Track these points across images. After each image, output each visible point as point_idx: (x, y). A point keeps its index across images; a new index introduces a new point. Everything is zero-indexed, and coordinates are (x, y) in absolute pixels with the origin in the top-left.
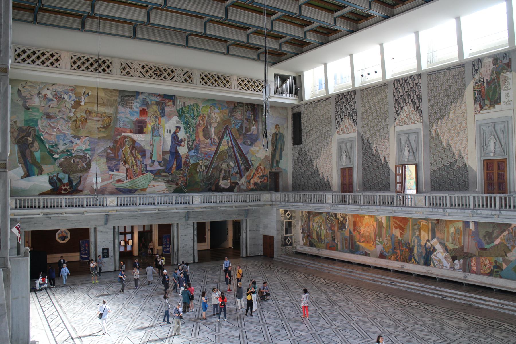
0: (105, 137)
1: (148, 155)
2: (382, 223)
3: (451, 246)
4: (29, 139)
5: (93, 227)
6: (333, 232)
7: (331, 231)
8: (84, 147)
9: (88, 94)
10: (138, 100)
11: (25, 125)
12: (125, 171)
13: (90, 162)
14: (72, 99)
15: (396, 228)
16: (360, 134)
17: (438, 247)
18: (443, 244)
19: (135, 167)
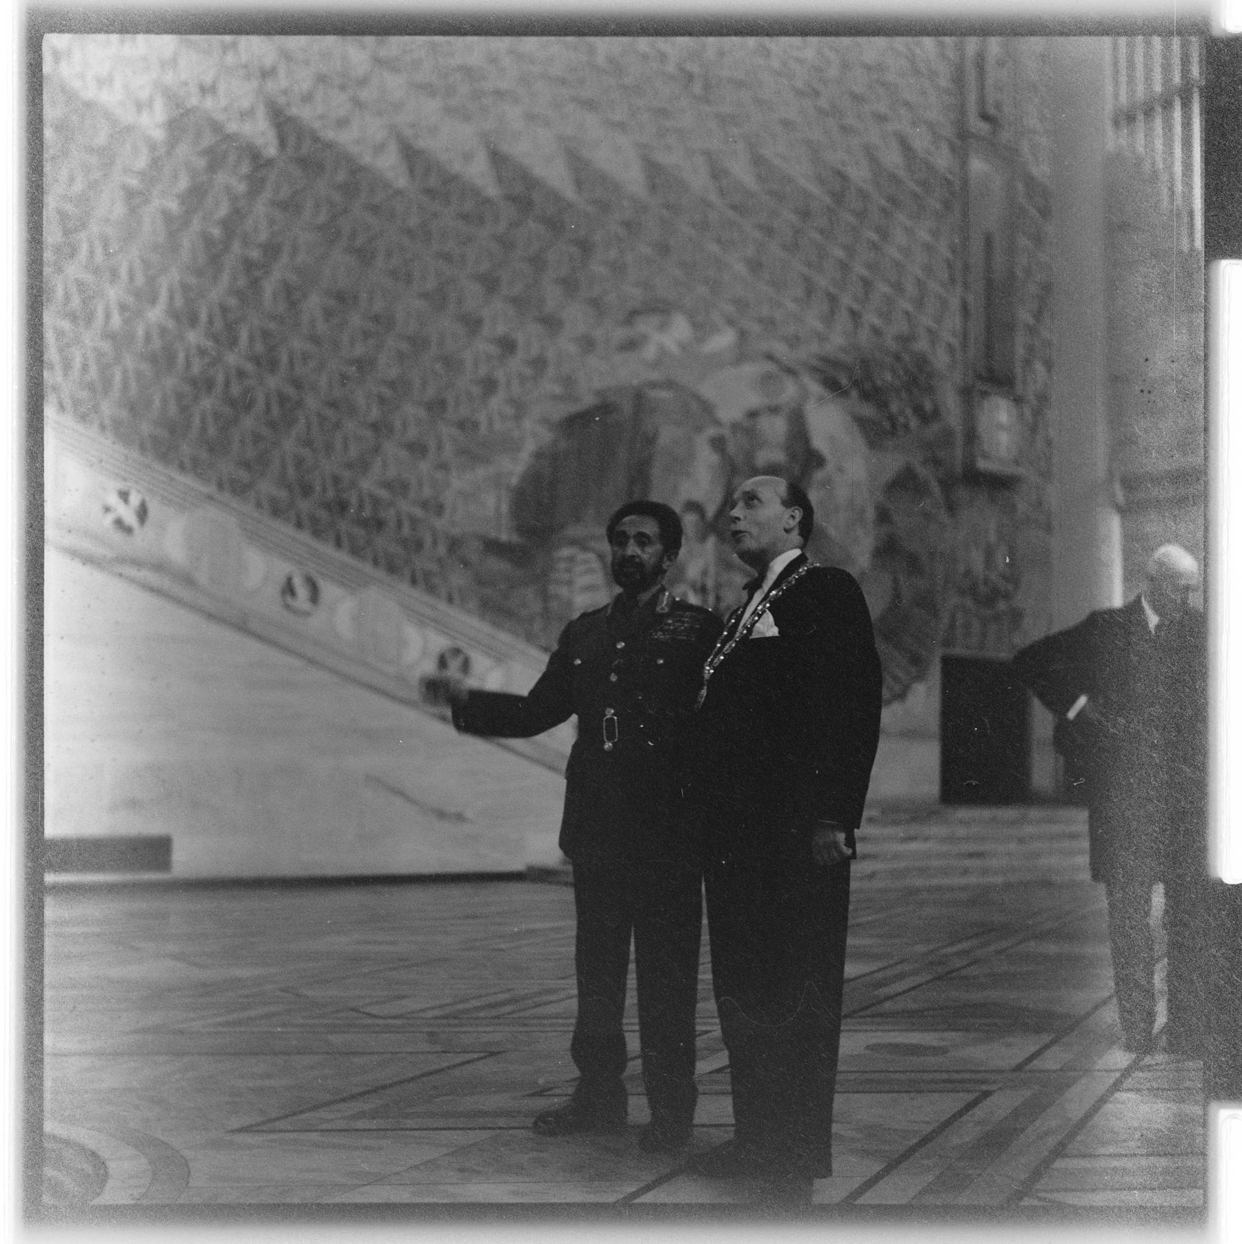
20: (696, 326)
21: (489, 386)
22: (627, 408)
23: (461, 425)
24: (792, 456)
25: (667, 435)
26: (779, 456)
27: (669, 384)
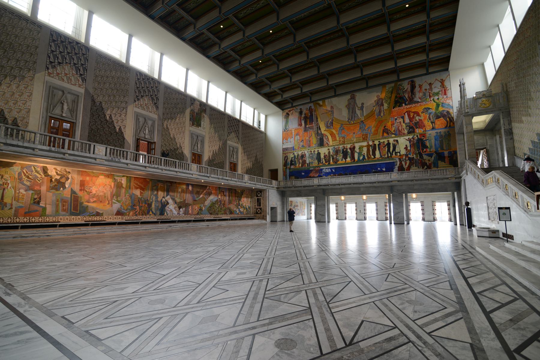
2: (122, 184)
3: (178, 200)
6: (39, 193)
7: (31, 192)
15: (136, 188)
16: (90, 94)
17: (170, 201)
18: (173, 199)
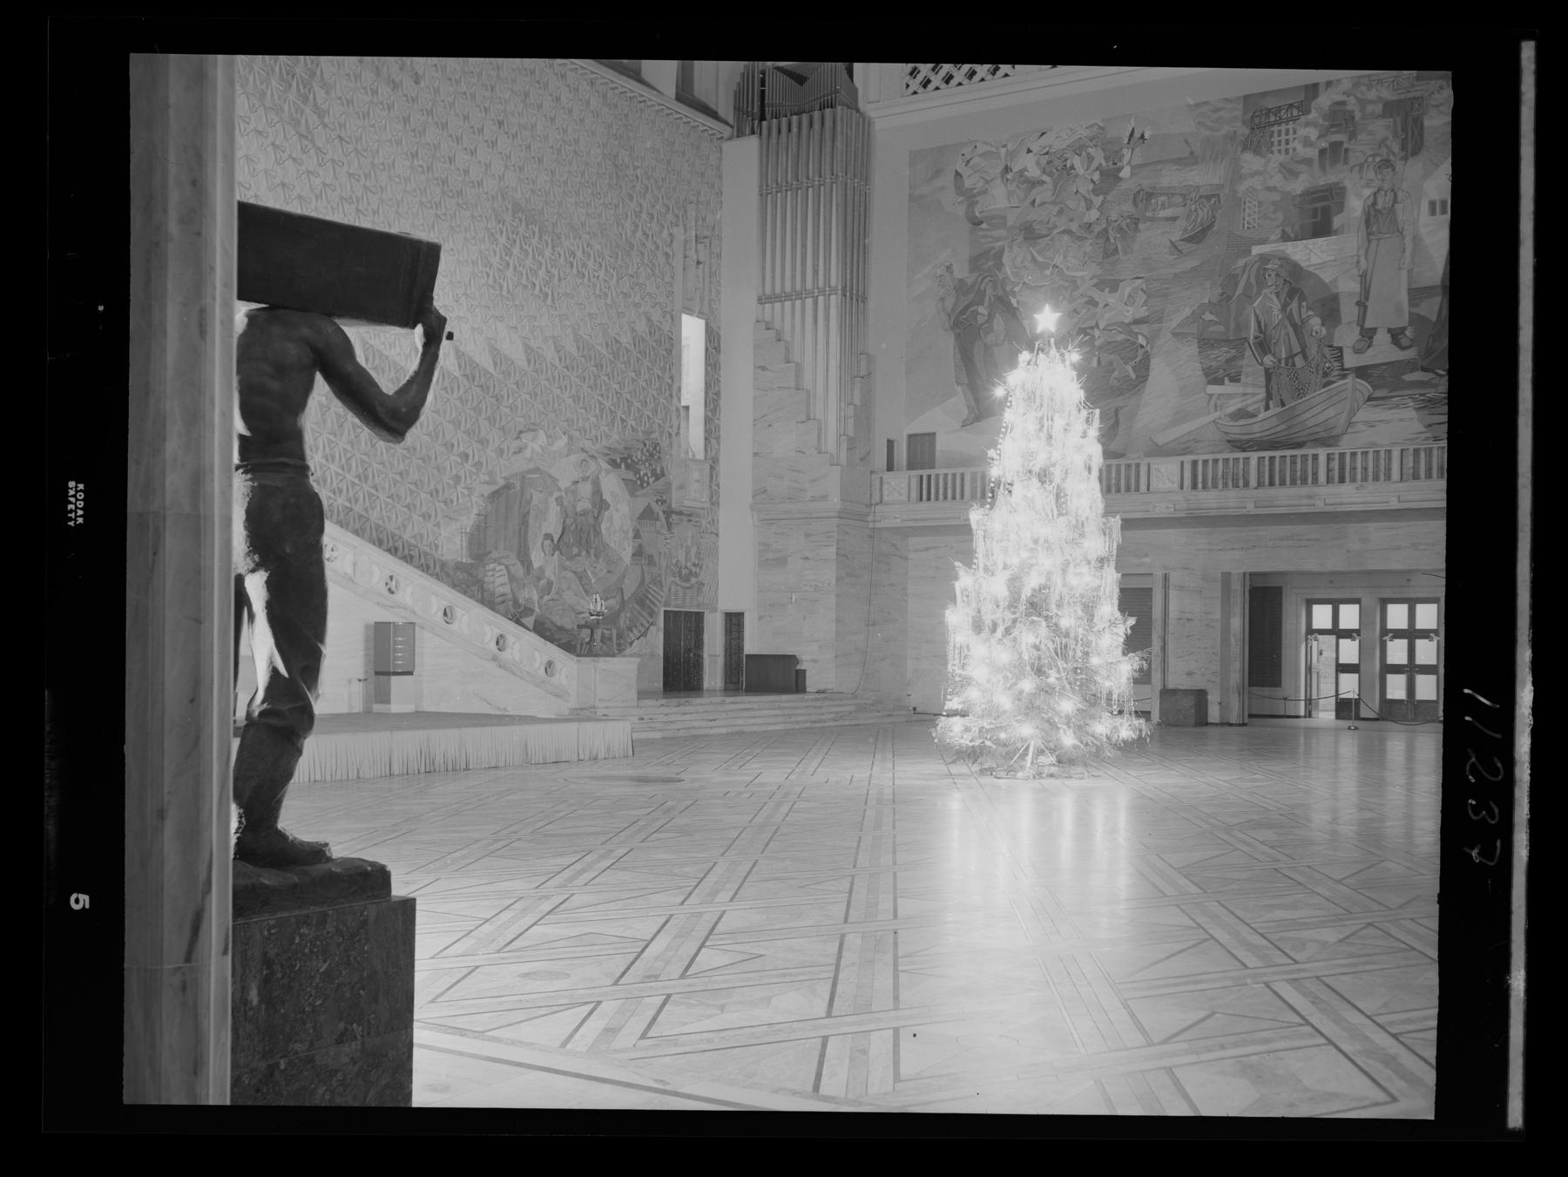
0: (1194, 269)
1: (1349, 311)
4: (981, 310)
5: (1159, 573)
8: (1130, 314)
9: (1142, 136)
10: (1313, 115)
11: (972, 270)
12: (1262, 380)
13: (1147, 358)
14: (1095, 165)
19: (1299, 362)
20: (549, 437)
21: (457, 479)
22: (518, 485)
23: (445, 502)
24: (594, 506)
25: (537, 498)
26: (588, 506)
27: (537, 470)
